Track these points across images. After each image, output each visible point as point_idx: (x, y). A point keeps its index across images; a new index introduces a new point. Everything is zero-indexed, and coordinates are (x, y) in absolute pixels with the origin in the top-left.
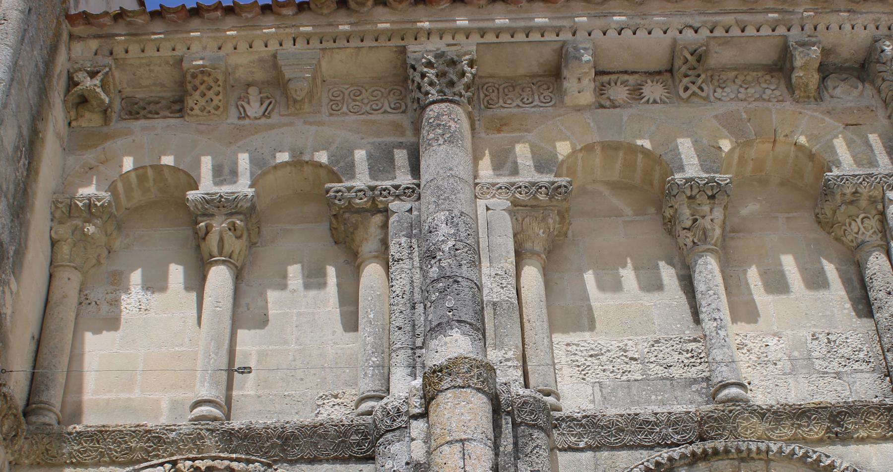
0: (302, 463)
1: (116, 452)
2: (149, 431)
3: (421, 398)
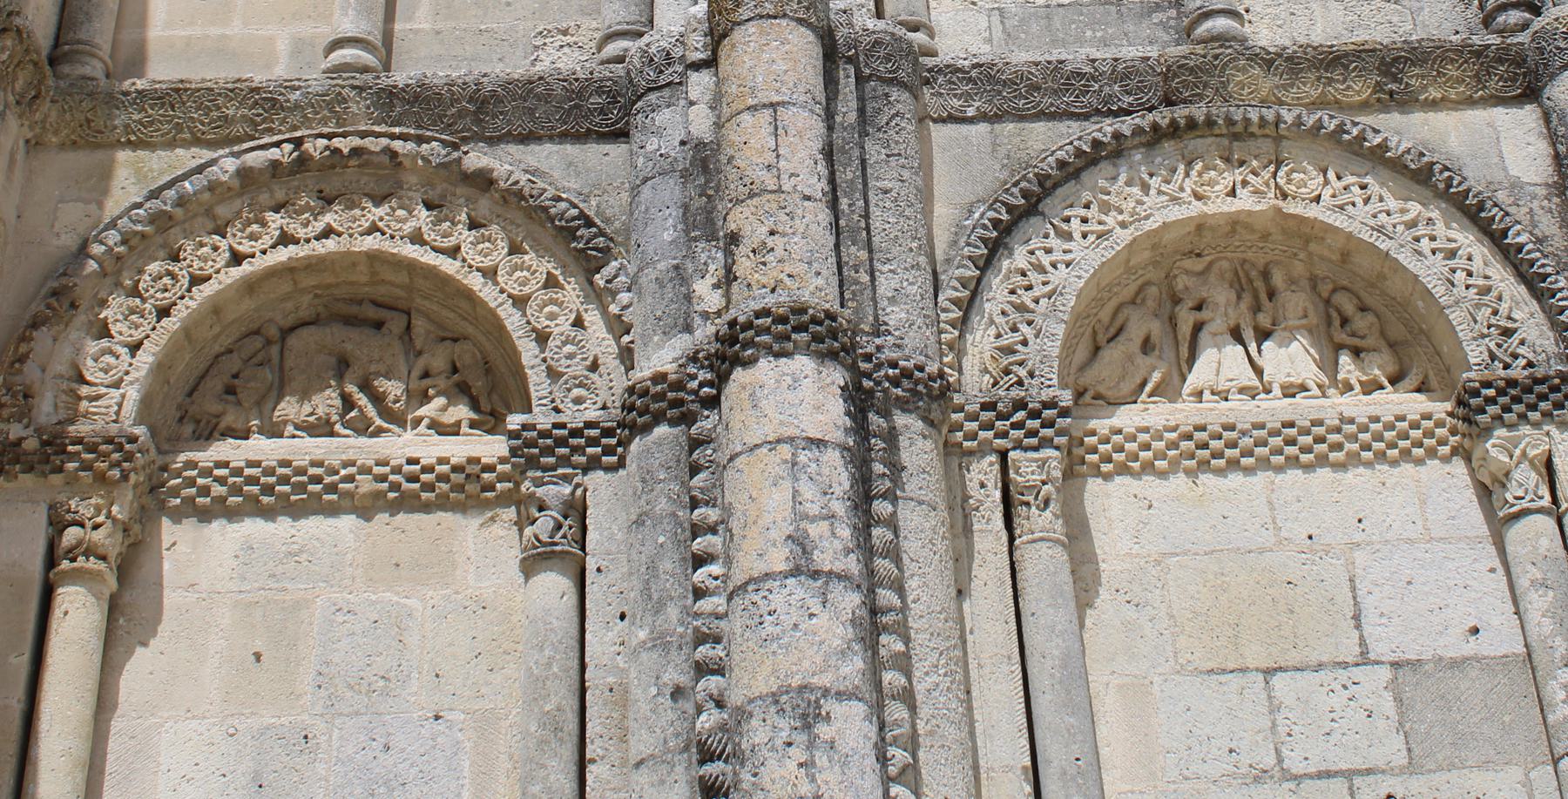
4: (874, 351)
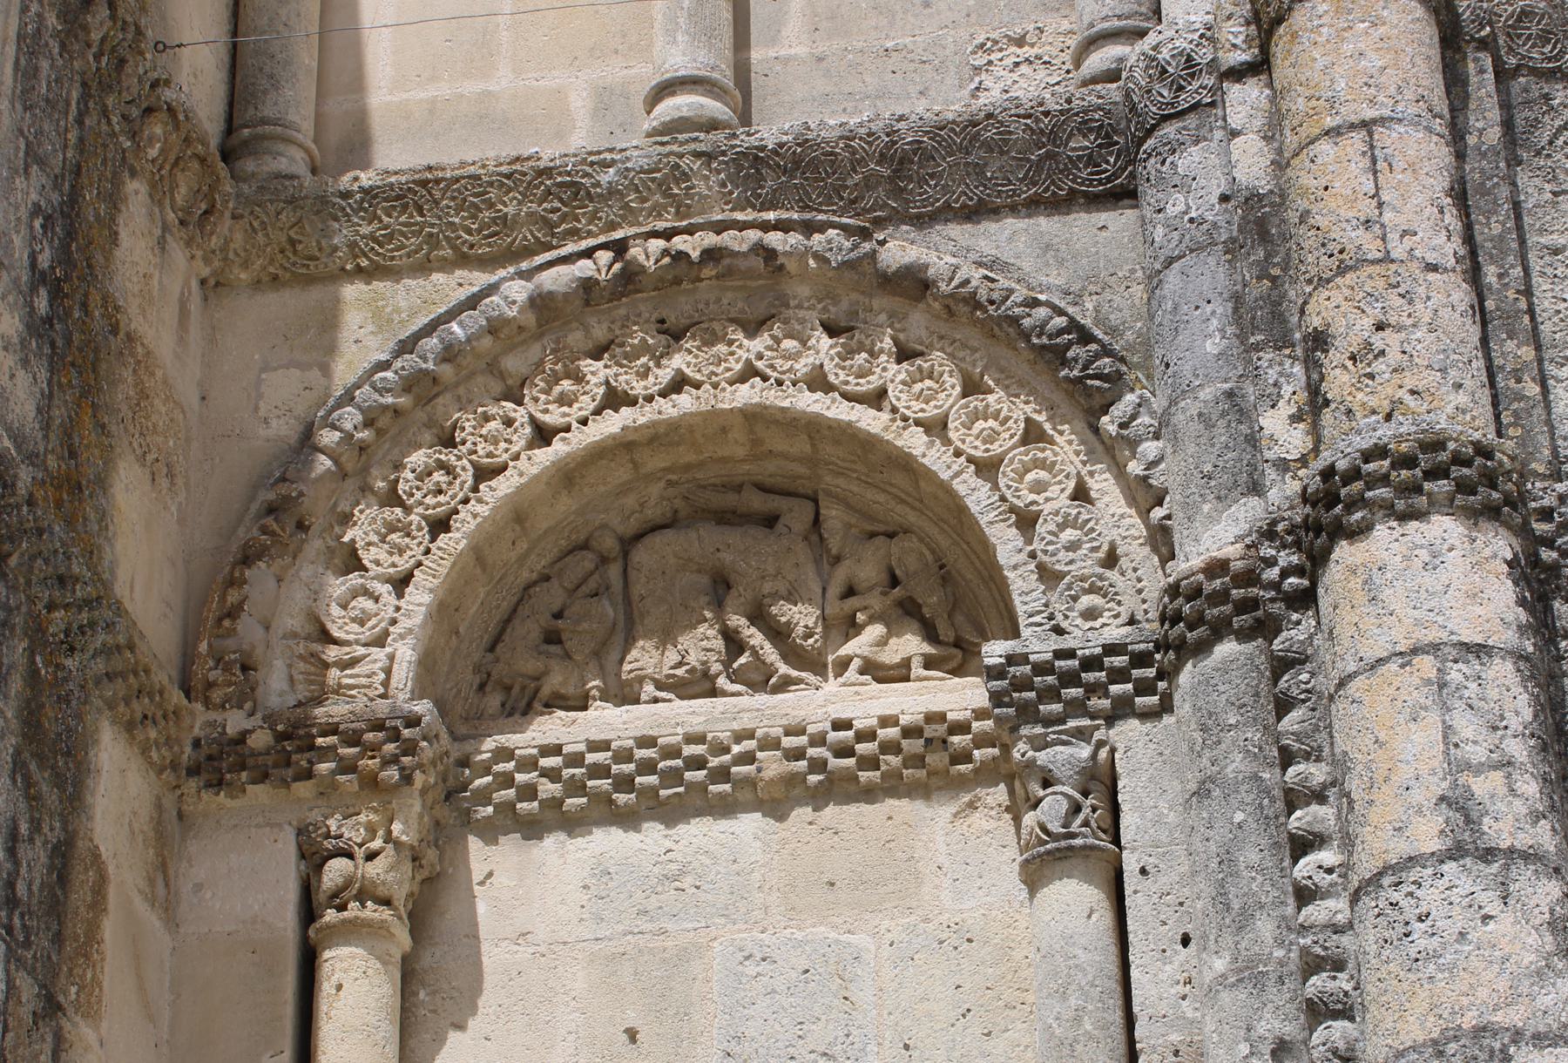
0: (947, 221)
1: (469, 232)
2: (547, 172)
3: (1248, 23)
4: (1555, 503)
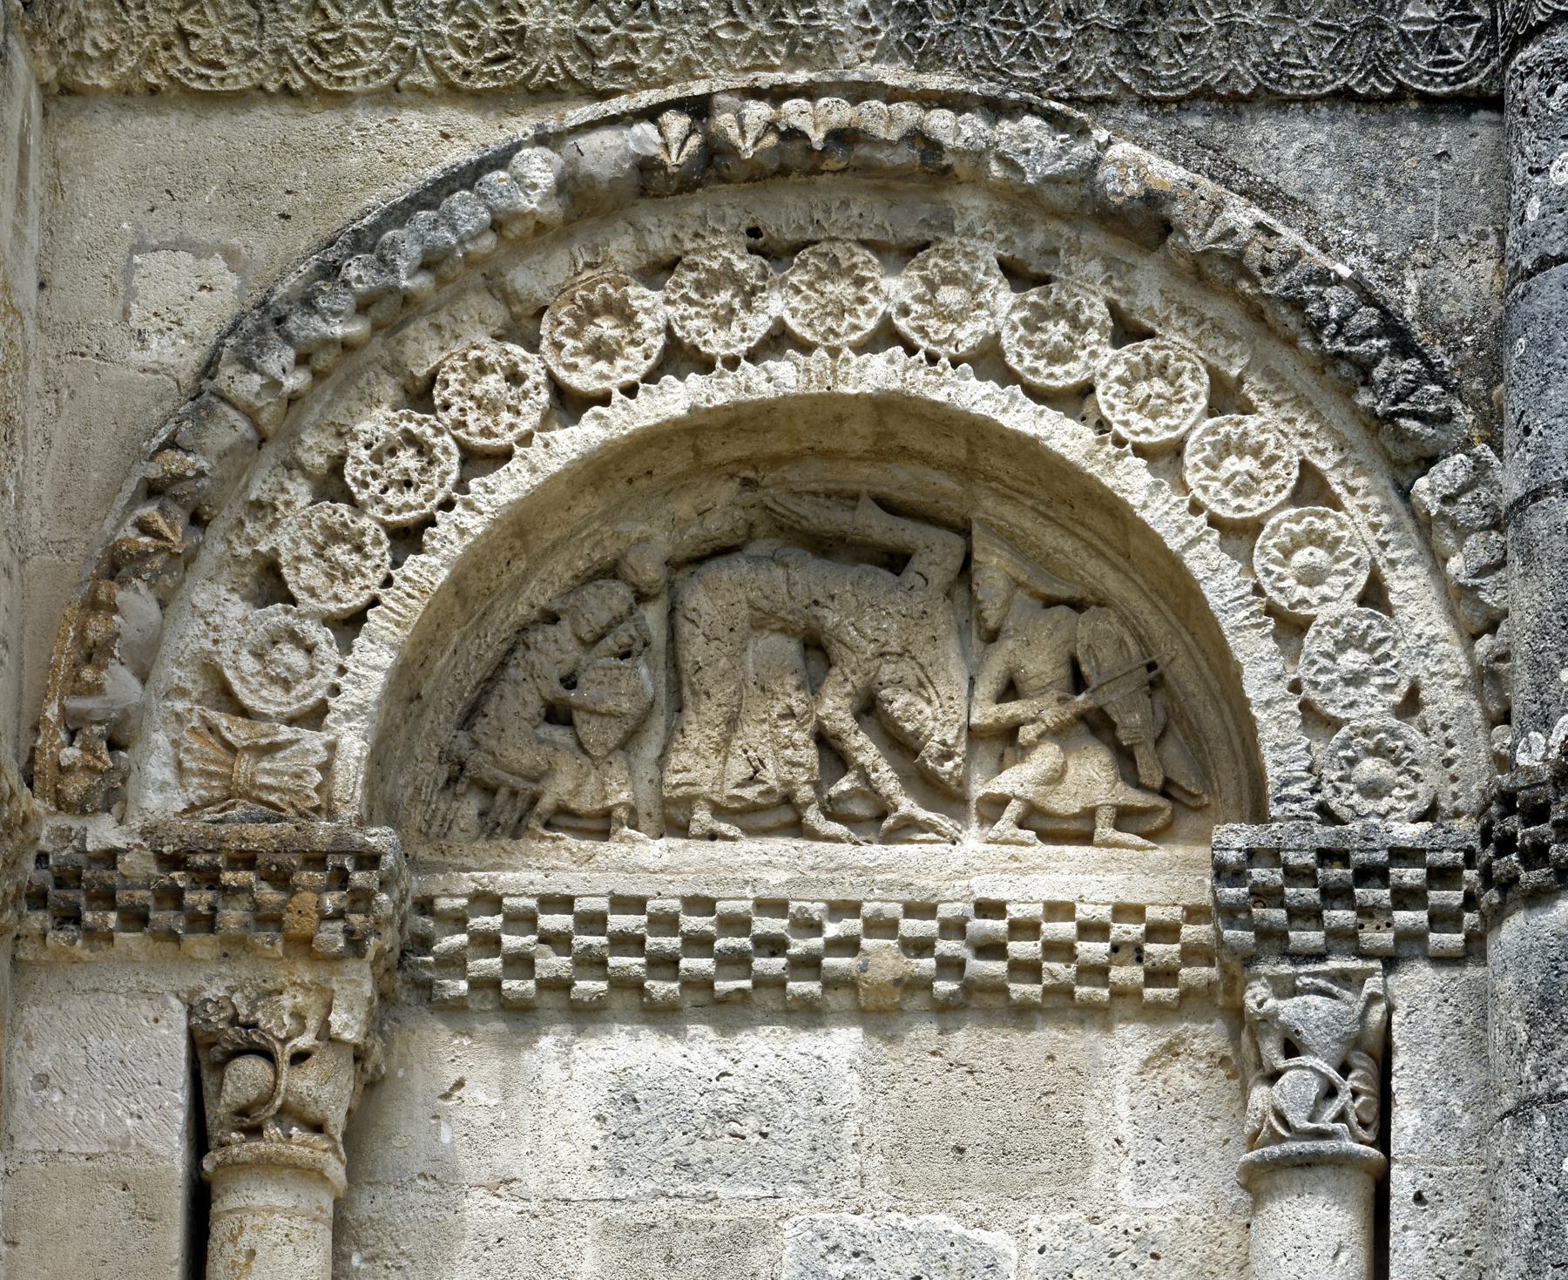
1: (464, 50)
